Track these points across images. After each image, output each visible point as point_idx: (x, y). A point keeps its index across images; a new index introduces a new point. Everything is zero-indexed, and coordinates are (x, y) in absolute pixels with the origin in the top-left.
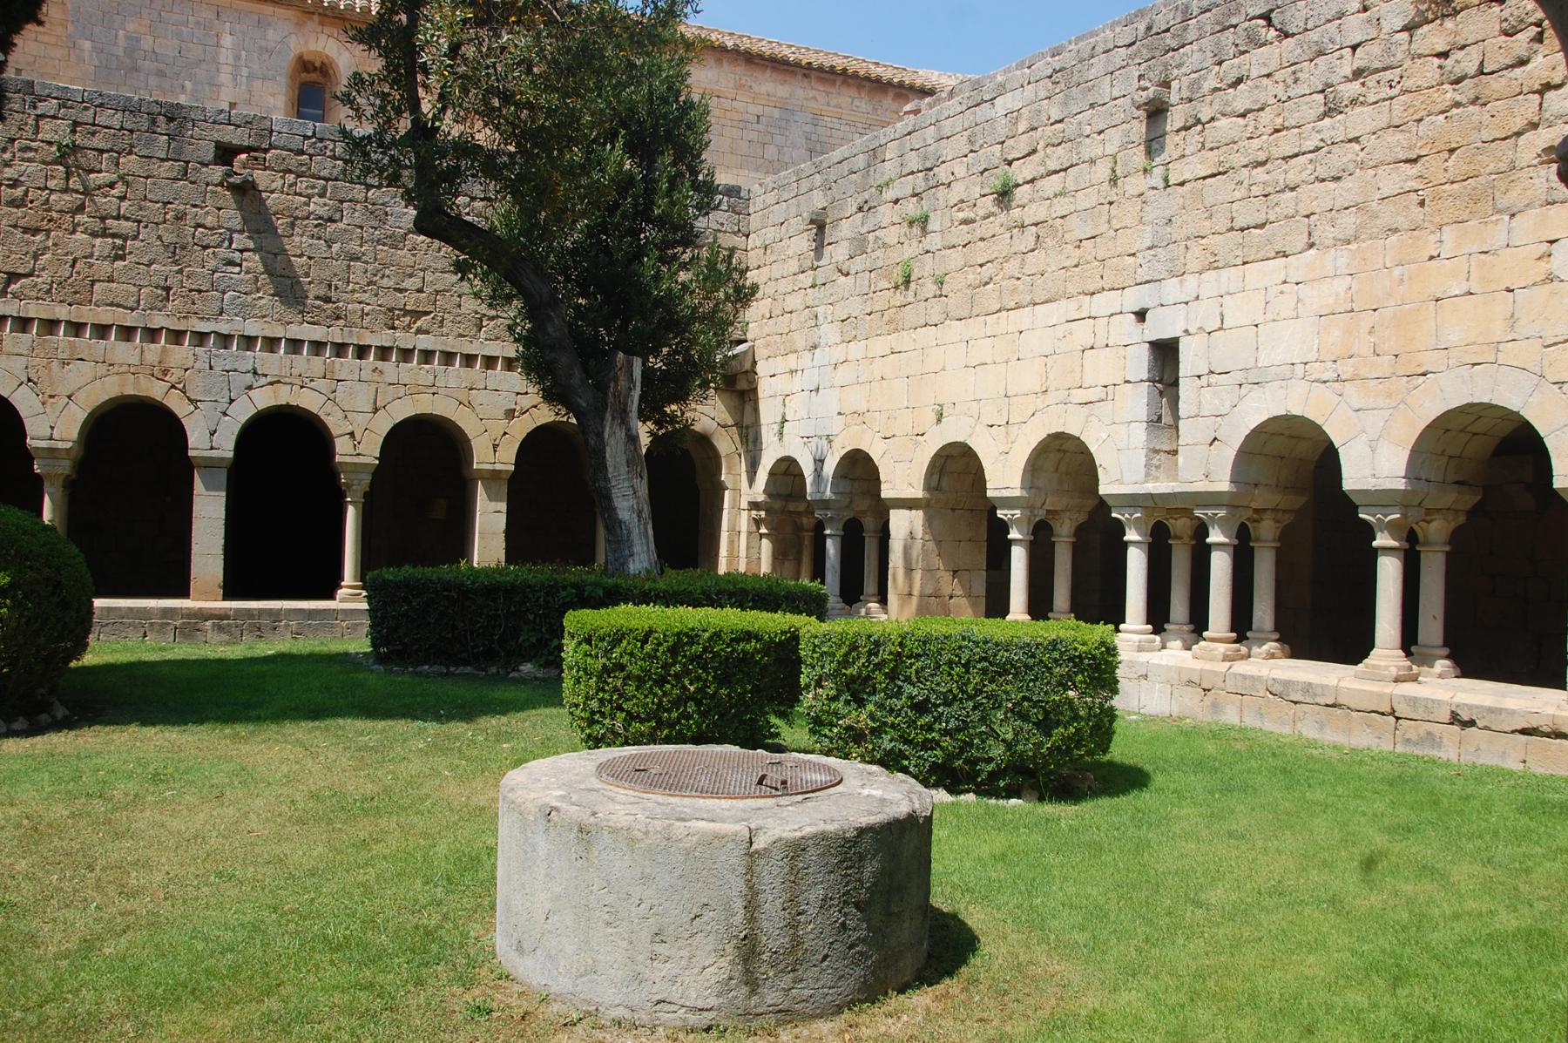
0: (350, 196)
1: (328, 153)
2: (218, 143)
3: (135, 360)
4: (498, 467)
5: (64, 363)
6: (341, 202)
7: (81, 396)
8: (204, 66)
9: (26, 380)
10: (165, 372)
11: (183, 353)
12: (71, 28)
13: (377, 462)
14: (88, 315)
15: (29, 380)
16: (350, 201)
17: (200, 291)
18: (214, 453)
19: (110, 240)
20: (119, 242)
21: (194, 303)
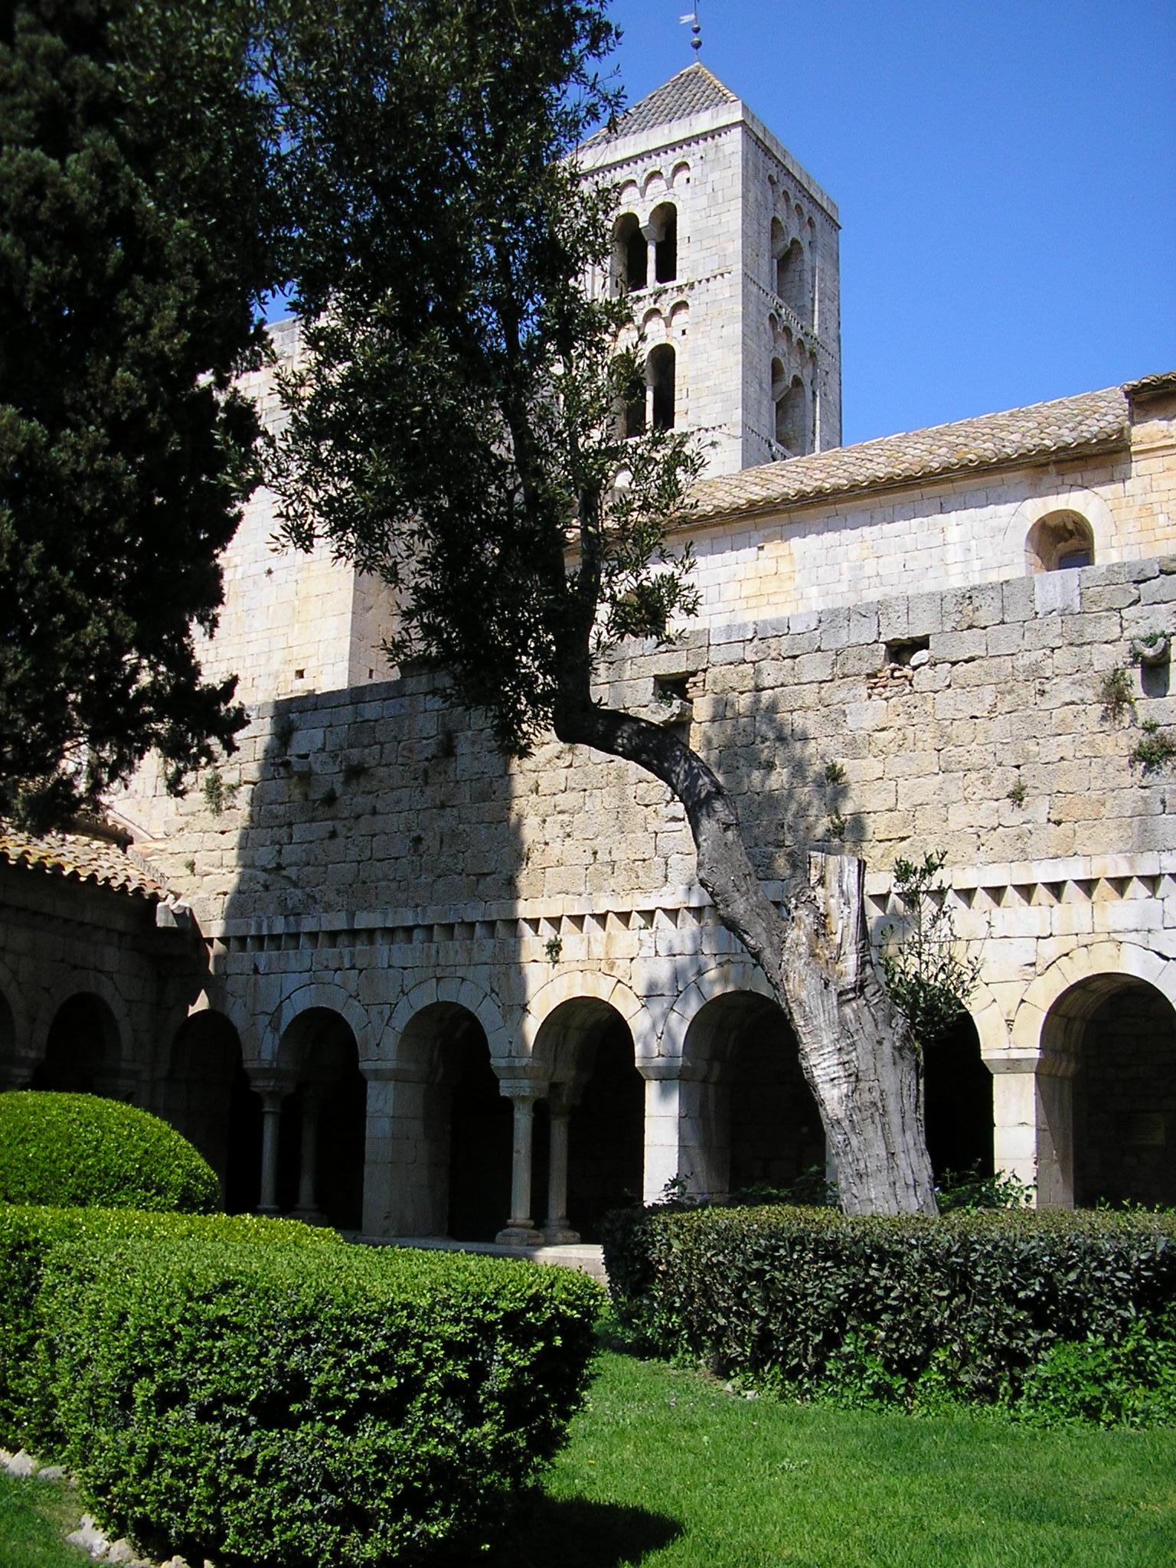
0: (800, 702)
1: (774, 654)
2: (655, 677)
3: (583, 956)
6: (792, 712)
8: (932, 573)
10: (612, 966)
12: (798, 577)
15: (493, 991)
16: (801, 708)
19: (561, 817)
20: (565, 817)
21: (638, 877)
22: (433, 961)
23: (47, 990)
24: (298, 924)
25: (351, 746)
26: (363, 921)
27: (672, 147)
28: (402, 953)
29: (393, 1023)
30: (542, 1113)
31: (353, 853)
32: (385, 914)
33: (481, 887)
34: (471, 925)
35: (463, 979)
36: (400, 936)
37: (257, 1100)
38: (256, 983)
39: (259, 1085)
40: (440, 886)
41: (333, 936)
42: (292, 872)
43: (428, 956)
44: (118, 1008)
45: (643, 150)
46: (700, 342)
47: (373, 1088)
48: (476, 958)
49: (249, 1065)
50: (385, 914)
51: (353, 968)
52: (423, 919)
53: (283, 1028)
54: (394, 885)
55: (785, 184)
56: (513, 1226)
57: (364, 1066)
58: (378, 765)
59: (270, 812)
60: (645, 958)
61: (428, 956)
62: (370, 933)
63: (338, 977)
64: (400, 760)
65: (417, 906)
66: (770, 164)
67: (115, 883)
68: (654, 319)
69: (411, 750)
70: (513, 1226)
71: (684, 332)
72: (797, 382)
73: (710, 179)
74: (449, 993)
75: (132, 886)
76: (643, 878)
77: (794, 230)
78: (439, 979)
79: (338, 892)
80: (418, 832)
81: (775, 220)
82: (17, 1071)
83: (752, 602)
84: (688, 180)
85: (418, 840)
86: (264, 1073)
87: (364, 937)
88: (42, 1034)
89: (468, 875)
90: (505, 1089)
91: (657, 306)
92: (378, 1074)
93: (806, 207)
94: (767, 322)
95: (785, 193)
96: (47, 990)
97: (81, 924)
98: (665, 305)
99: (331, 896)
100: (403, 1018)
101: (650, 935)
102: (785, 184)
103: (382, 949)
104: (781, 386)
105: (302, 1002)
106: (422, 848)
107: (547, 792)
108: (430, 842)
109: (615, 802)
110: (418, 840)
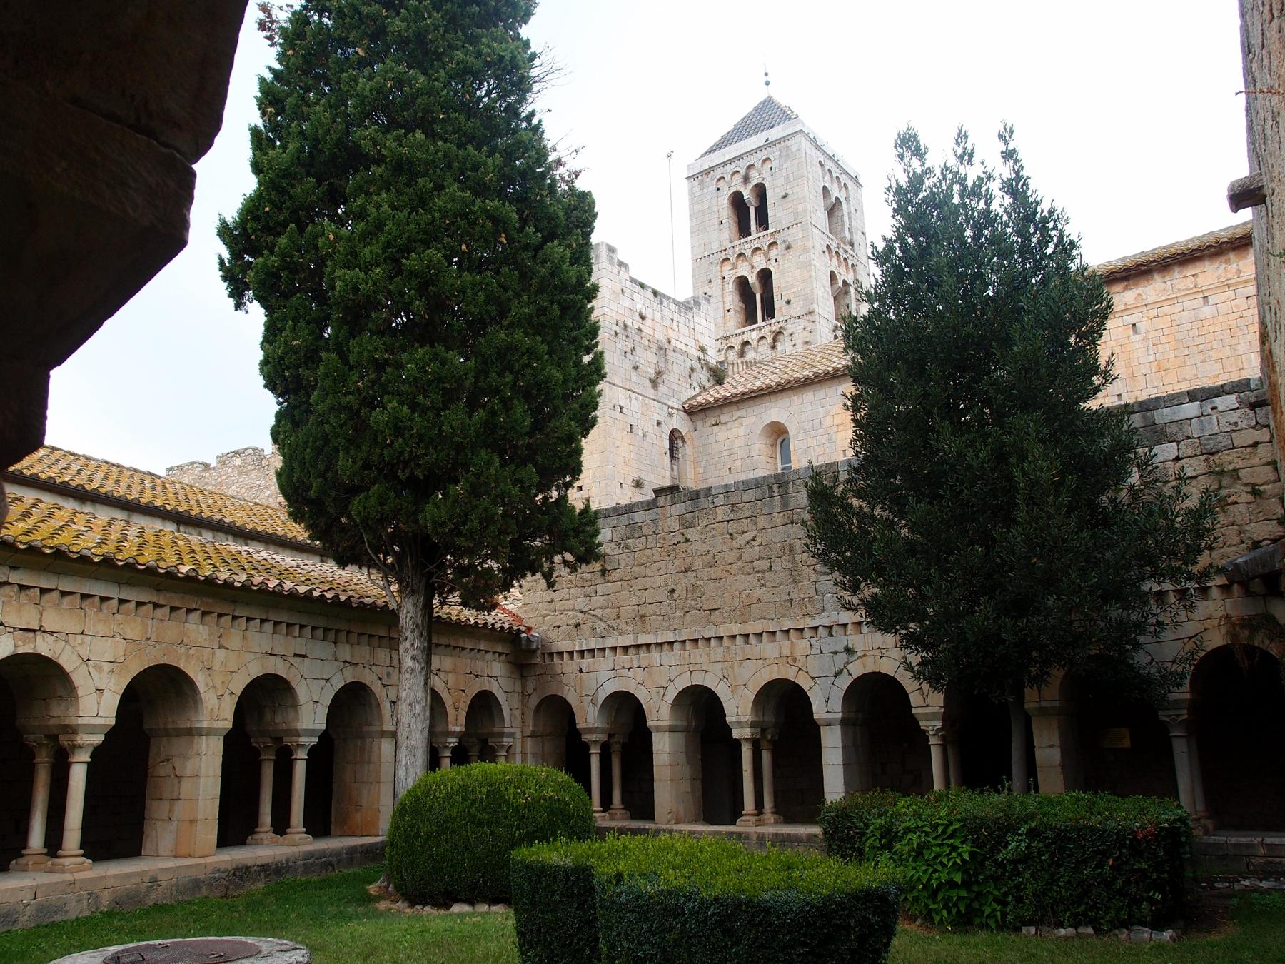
3: (776, 654)
4: (1044, 704)
5: (741, 662)
7: (750, 685)
9: (722, 677)
11: (802, 645)
13: (943, 710)
14: (751, 628)
17: (810, 598)
18: (830, 716)
20: (760, 575)
22: (687, 662)
23: (463, 691)
24: (604, 643)
25: (628, 538)
26: (643, 639)
27: (759, 149)
28: (667, 657)
29: (666, 698)
30: (756, 745)
31: (634, 600)
32: (657, 635)
33: (713, 617)
34: (709, 639)
35: (706, 671)
36: (666, 647)
37: (586, 746)
38: (581, 677)
39: (586, 738)
40: (688, 616)
41: (625, 648)
42: (598, 612)
43: (684, 658)
44: (501, 698)
45: (743, 152)
46: (787, 266)
47: (656, 737)
48: (712, 660)
49: (580, 724)
50: (657, 635)
51: (639, 667)
52: (680, 635)
53: (599, 704)
54: (660, 618)
55: (829, 165)
56: (746, 815)
57: (649, 724)
58: (646, 548)
59: (582, 578)
60: (814, 655)
61: (684, 658)
62: (648, 645)
63: (631, 673)
64: (658, 545)
65: (675, 629)
66: (819, 154)
67: (498, 626)
68: (758, 253)
69: (664, 539)
70: (746, 815)
71: (776, 260)
72: (845, 283)
73: (784, 167)
74: (698, 680)
75: (506, 626)
76: (809, 609)
77: (835, 192)
78: (691, 671)
79: (627, 623)
80: (673, 586)
81: (825, 188)
82: (449, 740)
83: (841, 428)
84: (771, 169)
85: (673, 591)
86: (591, 730)
87: (644, 648)
88: (463, 716)
89: (704, 610)
90: (736, 734)
91: (759, 246)
92: (658, 729)
93: (843, 178)
94: (825, 249)
95: (829, 170)
96: (463, 691)
97: (479, 651)
98: (764, 244)
99: (623, 626)
100: (671, 695)
101: (817, 641)
102: (829, 165)
103: (656, 657)
104: (836, 287)
105: (610, 688)
106: (676, 595)
107: (748, 560)
108: (680, 592)
109: (789, 565)
110: (673, 591)
